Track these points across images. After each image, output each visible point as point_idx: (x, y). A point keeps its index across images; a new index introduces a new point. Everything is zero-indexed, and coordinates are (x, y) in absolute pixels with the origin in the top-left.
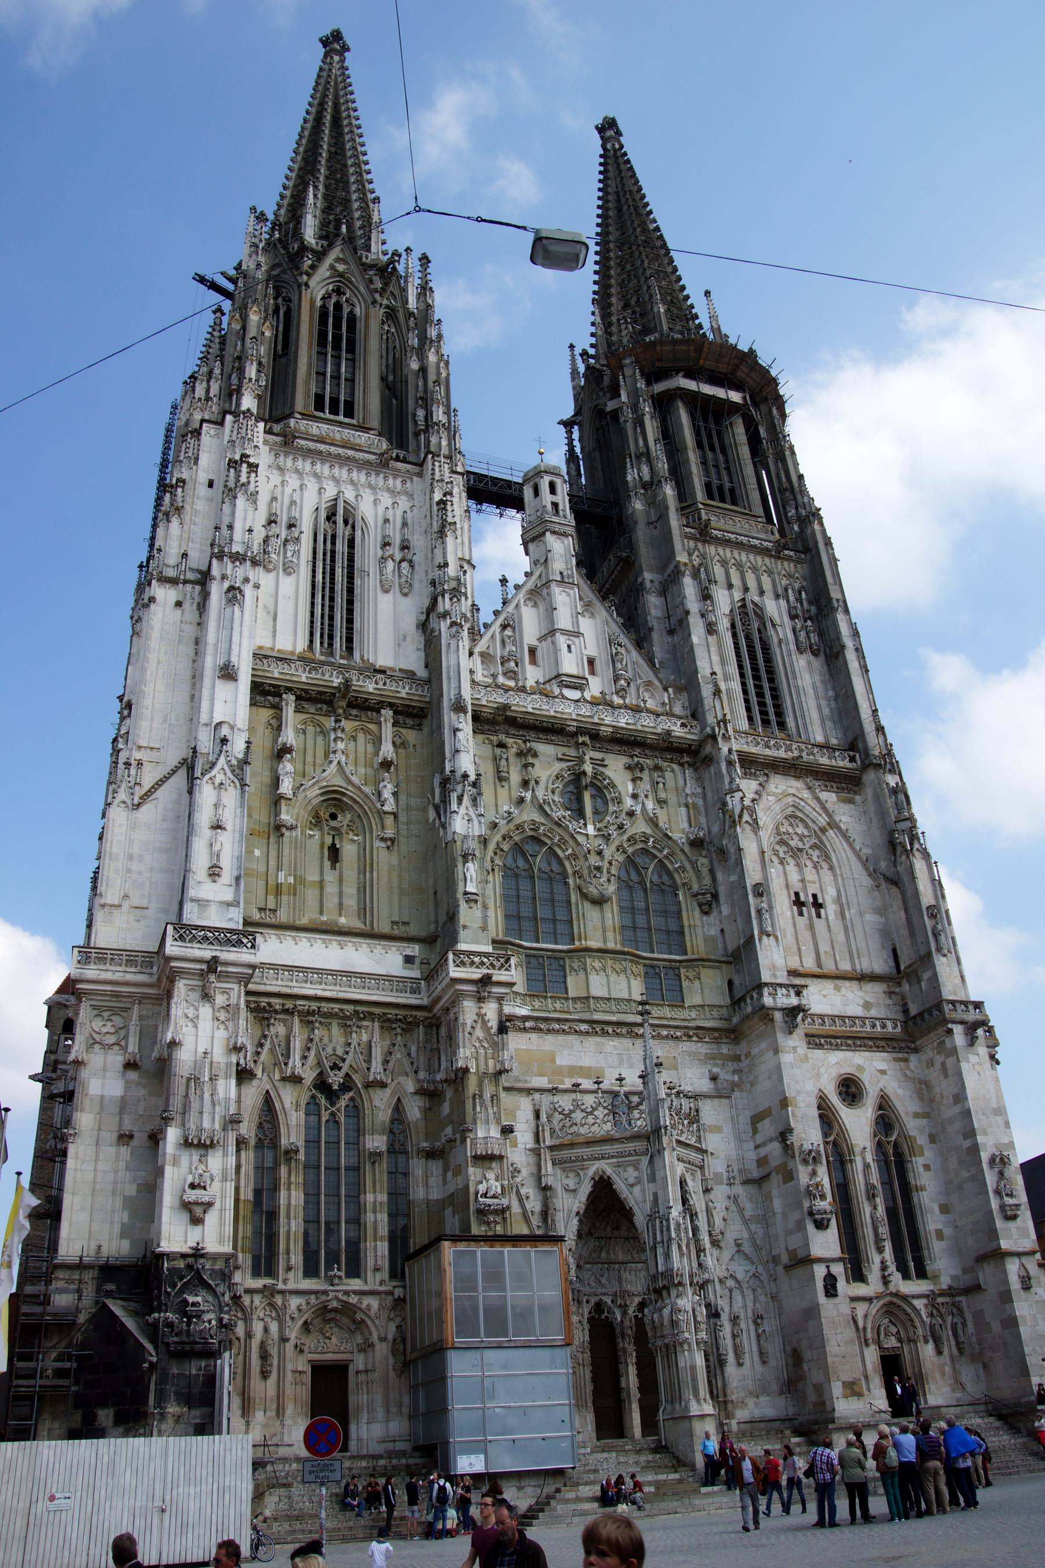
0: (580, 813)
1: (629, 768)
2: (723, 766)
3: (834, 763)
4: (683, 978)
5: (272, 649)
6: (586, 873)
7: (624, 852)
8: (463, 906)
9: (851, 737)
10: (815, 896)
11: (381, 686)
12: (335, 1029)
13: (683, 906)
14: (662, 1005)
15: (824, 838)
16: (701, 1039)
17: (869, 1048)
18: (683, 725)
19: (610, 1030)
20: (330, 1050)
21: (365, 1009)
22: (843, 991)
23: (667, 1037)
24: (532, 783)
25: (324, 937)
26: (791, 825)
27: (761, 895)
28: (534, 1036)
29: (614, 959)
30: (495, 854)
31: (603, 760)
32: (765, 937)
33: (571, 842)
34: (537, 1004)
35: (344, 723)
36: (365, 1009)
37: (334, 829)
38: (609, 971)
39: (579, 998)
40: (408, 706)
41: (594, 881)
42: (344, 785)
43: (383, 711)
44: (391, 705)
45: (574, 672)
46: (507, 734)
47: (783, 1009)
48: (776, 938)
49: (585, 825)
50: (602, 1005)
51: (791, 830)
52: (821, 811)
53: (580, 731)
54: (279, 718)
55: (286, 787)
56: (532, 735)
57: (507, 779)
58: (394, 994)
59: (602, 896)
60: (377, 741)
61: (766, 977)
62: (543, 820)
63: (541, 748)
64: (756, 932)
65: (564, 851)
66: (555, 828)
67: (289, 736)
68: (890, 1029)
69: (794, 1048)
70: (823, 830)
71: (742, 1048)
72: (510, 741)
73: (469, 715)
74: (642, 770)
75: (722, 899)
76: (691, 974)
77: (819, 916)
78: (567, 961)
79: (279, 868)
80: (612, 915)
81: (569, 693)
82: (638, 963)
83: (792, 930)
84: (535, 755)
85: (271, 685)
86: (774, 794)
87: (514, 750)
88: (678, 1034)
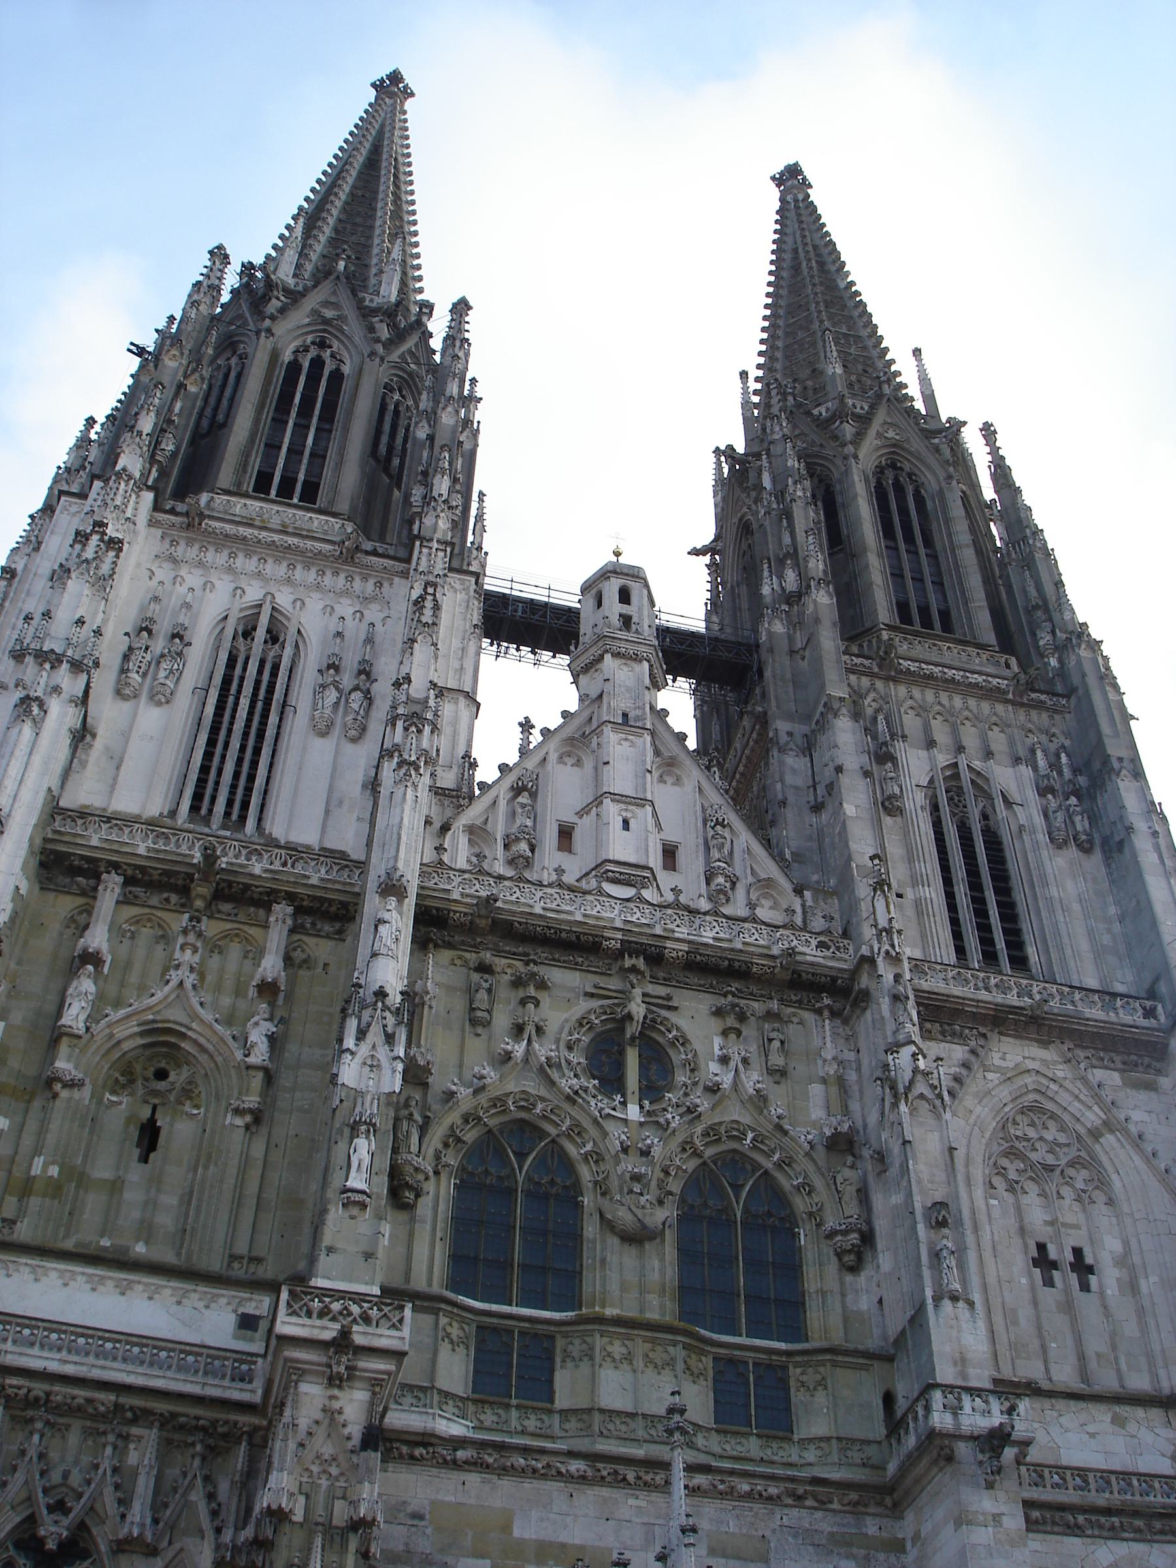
0: (613, 1083)
1: (718, 1013)
2: (885, 1004)
3: (1112, 1017)
4: (792, 1383)
5: (105, 810)
6: (614, 1183)
7: (696, 1154)
8: (336, 1214)
9: (1148, 978)
10: (1078, 1252)
11: (277, 866)
12: (74, 1438)
14: (743, 1435)
15: (1097, 1147)
16: (822, 1504)
18: (821, 945)
19: (631, 1476)
20: (56, 1477)
22: (1132, 1427)
23: (748, 1496)
24: (530, 1029)
25: (90, 1270)
26: (1032, 1124)
27: (942, 1224)
28: (474, 1479)
29: (653, 1341)
30: (446, 1145)
32: (947, 1304)
33: (593, 1132)
34: (489, 1418)
35: (205, 924)
37: (155, 1093)
38: (639, 1363)
39: (575, 1411)
40: (322, 900)
41: (628, 1199)
42: (184, 1019)
43: (276, 907)
44: (291, 897)
46: (498, 952)
47: (973, 1438)
48: (971, 1304)
49: (624, 1104)
50: (617, 1425)
51: (1031, 1133)
52: (1090, 1101)
53: (629, 948)
54: (88, 910)
55: (75, 1016)
56: (542, 953)
57: (487, 1024)
58: (200, 1378)
59: (644, 1227)
60: (256, 954)
61: (945, 1373)
62: (543, 1092)
63: (557, 976)
64: (929, 1293)
65: (580, 1146)
66: (566, 1106)
67: (98, 938)
70: (1095, 1134)
71: (905, 1528)
72: (500, 963)
73: (410, 902)
74: (742, 1017)
75: (881, 1243)
76: (810, 1377)
77: (1085, 1287)
78: (560, 1343)
79: (37, 1152)
82: (703, 1352)
85: (82, 857)
86: (998, 1070)
87: (507, 978)
88: (773, 1491)
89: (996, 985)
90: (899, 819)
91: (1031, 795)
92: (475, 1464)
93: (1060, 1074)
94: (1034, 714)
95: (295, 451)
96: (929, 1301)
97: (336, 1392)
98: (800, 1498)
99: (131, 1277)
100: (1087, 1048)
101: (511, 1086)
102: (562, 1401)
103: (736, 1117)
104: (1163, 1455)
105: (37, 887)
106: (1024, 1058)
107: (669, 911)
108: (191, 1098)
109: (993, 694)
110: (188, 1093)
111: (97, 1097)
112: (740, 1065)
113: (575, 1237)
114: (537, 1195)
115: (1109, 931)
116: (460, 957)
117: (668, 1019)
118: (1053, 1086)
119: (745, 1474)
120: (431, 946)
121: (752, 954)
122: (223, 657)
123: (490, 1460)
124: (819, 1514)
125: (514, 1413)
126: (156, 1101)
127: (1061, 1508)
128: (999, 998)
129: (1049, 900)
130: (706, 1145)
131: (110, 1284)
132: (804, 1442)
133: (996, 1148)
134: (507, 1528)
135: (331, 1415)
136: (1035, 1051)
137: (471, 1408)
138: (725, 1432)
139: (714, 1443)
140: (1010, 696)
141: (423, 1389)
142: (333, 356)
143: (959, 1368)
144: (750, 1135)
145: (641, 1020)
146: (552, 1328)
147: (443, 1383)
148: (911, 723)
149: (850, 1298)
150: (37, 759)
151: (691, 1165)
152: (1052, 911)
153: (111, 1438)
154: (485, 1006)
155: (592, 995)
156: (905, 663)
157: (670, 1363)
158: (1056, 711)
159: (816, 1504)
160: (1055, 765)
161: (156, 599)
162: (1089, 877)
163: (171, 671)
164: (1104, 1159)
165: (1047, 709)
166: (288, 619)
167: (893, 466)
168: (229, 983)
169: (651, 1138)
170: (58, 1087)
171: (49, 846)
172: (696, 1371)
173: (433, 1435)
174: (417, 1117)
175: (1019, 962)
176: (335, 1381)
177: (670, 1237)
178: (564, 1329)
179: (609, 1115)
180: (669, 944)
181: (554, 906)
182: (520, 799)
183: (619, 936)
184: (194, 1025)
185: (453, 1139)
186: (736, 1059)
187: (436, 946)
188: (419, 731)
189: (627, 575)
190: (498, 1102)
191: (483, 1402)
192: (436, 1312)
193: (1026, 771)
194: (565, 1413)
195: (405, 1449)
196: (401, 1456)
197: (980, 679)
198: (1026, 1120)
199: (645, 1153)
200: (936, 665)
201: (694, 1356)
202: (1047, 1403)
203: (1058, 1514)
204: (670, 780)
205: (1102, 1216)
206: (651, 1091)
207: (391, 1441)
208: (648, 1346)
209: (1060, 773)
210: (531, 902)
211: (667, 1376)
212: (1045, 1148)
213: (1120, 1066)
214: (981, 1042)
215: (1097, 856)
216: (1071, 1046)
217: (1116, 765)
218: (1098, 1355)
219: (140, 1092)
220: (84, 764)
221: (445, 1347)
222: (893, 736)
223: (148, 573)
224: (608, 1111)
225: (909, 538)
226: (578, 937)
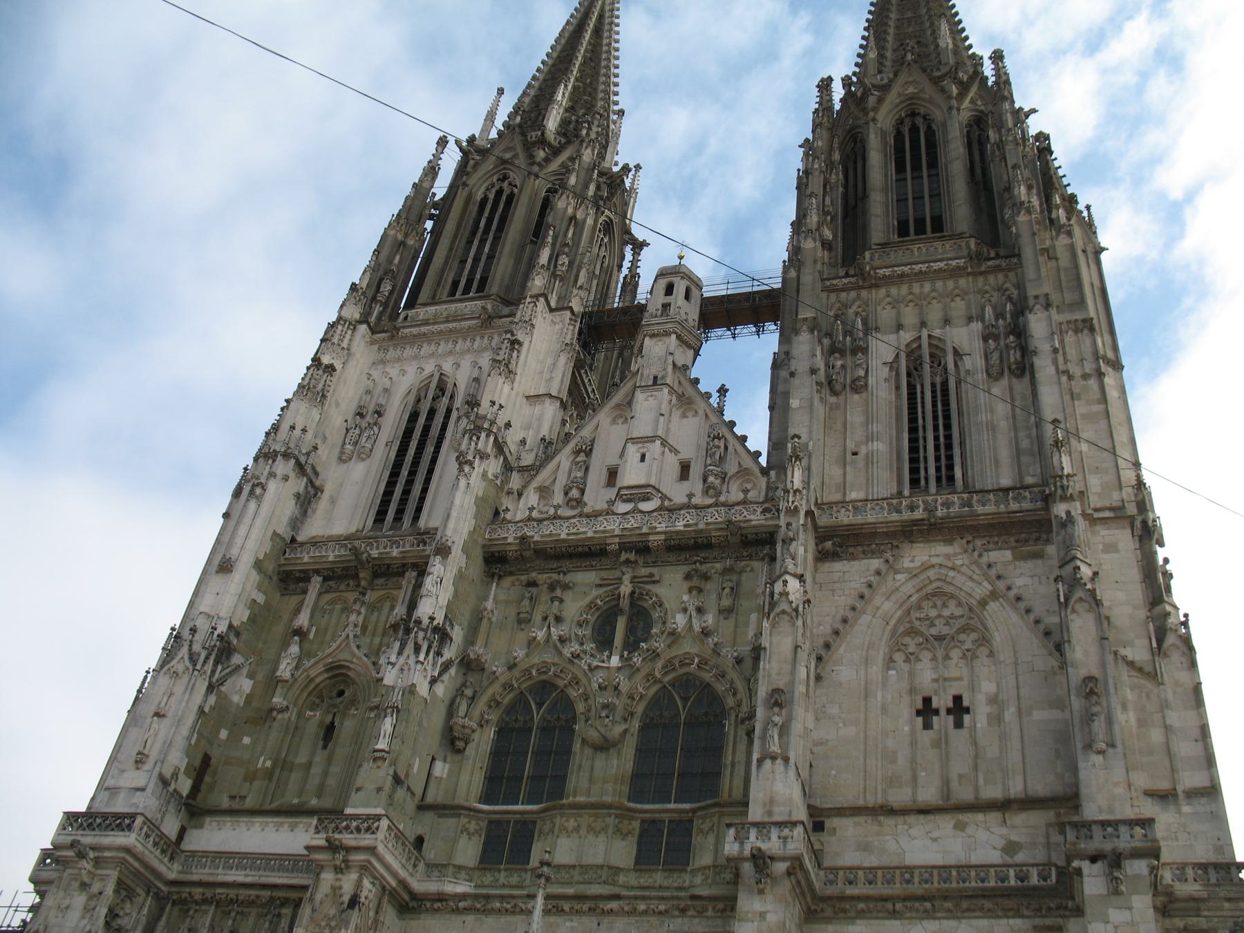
7: (656, 681)
10: (958, 699)
11: (408, 548)
16: (701, 913)
17: (989, 914)
18: (764, 511)
19: (566, 908)
21: (282, 894)
22: (970, 830)
23: (645, 912)
25: (275, 820)
26: (935, 606)
27: (777, 704)
29: (597, 816)
31: (652, 575)
34: (488, 879)
36: (282, 894)
38: (583, 831)
45: (642, 481)
46: (542, 571)
49: (609, 657)
50: (564, 875)
51: (933, 613)
53: (624, 547)
54: (302, 603)
55: (285, 669)
62: (556, 660)
64: (755, 756)
66: (569, 666)
67: (303, 620)
68: (1034, 880)
69: (762, 915)
70: (983, 603)
74: (706, 577)
77: (959, 724)
78: (538, 826)
80: (622, 762)
81: (623, 507)
82: (632, 818)
84: (566, 587)
85: (300, 571)
86: (908, 570)
88: (662, 908)
90: (864, 395)
91: (978, 345)
92: (471, 909)
93: (958, 562)
94: (991, 278)
95: (476, 260)
96: (755, 762)
97: (340, 876)
98: (683, 911)
99: (297, 820)
100: (985, 536)
101: (536, 660)
103: (687, 650)
104: (995, 848)
105: (278, 595)
106: (930, 556)
107: (655, 514)
108: (353, 705)
109: (954, 273)
110: (353, 702)
111: (300, 715)
112: (694, 614)
113: (568, 752)
114: (546, 729)
115: (1029, 436)
116: (518, 580)
117: (649, 590)
118: (951, 574)
119: (643, 898)
120: (496, 577)
121: (711, 530)
122: (406, 417)
123: (478, 906)
124: (697, 920)
125: (503, 873)
126: (335, 710)
127: (884, 899)
128: (906, 515)
131: (271, 825)
132: (694, 872)
133: (901, 629)
135: (336, 890)
136: (942, 549)
137: (477, 874)
138: (641, 871)
139: (633, 879)
140: (969, 270)
141: (444, 866)
142: (510, 184)
143: (767, 808)
144: (696, 660)
145: (627, 594)
146: (535, 816)
147: (459, 860)
148: (885, 315)
150: (259, 522)
151: (653, 691)
153: (269, 917)
154: (528, 609)
155: (601, 586)
156: (881, 272)
157: (604, 829)
158: (1009, 270)
159: (695, 913)
160: (999, 315)
161: (368, 392)
163: (369, 437)
164: (989, 623)
165: (1002, 270)
166: (448, 377)
167: (913, 114)
168: (380, 630)
170: (275, 713)
171: (281, 569)
172: (625, 831)
173: (444, 894)
175: (946, 479)
176: (338, 870)
178: (542, 815)
179: (597, 667)
180: (651, 538)
181: (575, 531)
183: (617, 540)
184: (354, 660)
185: (494, 703)
186: (692, 609)
187: (500, 577)
188: (478, 438)
189: (671, 274)
190: (527, 671)
191: (485, 869)
192: (459, 816)
193: (977, 326)
195: (428, 905)
196: (427, 910)
197: (942, 265)
198: (931, 604)
199: (616, 688)
200: (906, 265)
201: (626, 822)
202: (900, 819)
203: (880, 904)
204: (690, 414)
206: (631, 645)
207: (422, 900)
208: (592, 819)
209: (1004, 319)
210: (559, 532)
211: (602, 838)
212: (943, 621)
213: (1014, 544)
216: (970, 538)
217: (1031, 302)
218: (960, 776)
219: (325, 705)
220: (314, 511)
222: (867, 330)
223: (366, 376)
224: (595, 663)
225: (916, 167)
226: (590, 548)
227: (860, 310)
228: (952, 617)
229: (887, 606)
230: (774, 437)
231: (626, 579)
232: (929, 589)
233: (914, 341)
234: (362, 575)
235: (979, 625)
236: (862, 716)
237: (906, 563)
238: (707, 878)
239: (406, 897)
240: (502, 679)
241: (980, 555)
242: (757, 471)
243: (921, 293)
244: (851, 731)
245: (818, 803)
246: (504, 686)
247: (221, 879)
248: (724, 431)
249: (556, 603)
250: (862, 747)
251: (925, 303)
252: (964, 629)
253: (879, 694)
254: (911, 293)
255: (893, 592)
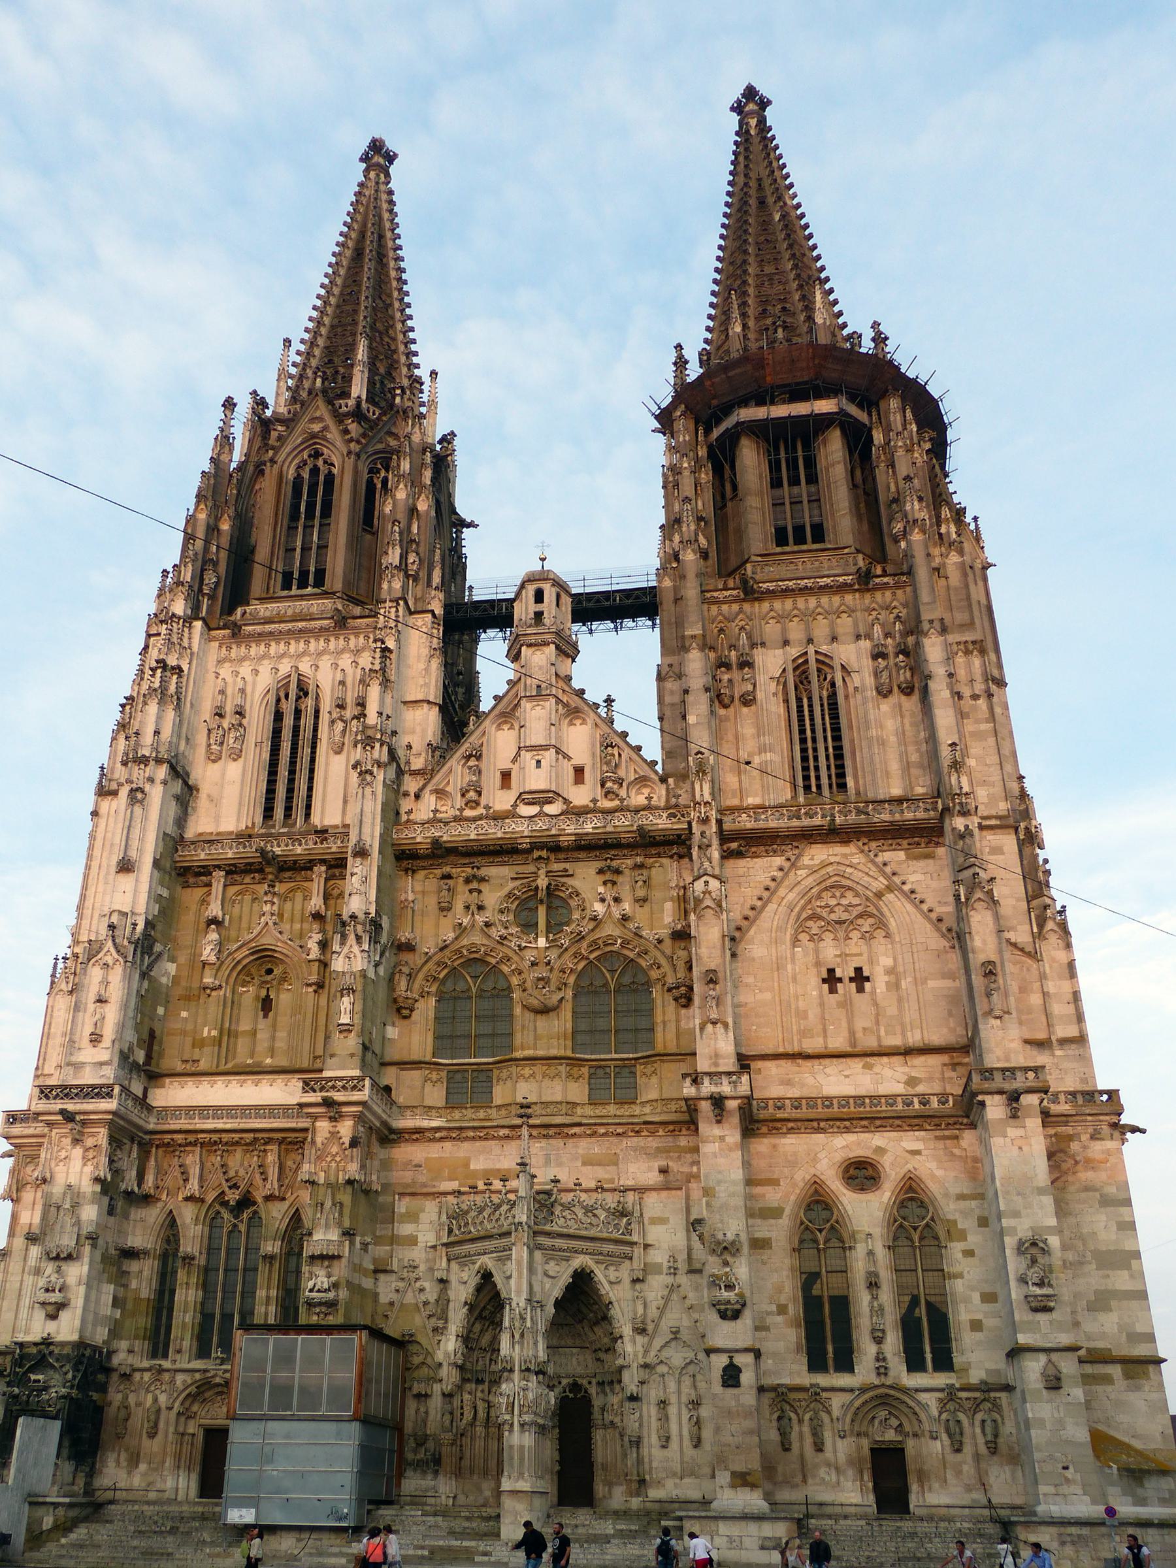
13: (659, 1002)
26: (834, 896)
46: (455, 866)
62: (485, 942)
66: (499, 947)
70: (879, 895)
77: (861, 990)
78: (496, 1072)
80: (563, 1021)
83: (818, 1010)
89: (806, 814)
91: (867, 663)
93: (855, 861)
101: (465, 942)
102: (498, 1100)
118: (849, 870)
120: (410, 873)
123: (454, 1135)
129: (870, 739)
130: (591, 952)
132: (643, 1103)
134: (467, 1165)
139: (588, 1110)
149: (683, 1024)
152: (870, 747)
162: (907, 714)
164: (885, 910)
169: (553, 955)
174: (406, 970)
177: (568, 1007)
182: (470, 763)
187: (414, 871)
192: (421, 1069)
193: (866, 645)
194: (499, 1107)
205: (880, 944)
214: (796, 852)
215: (916, 697)
221: (428, 1085)
227: (743, 623)
228: (850, 905)
229: (791, 896)
230: (666, 746)
231: (542, 872)
232: (828, 883)
233: (800, 656)
234: (268, 870)
235: (875, 912)
236: (776, 984)
237: (806, 860)
238: (655, 1109)
239: (386, 1132)
240: (436, 958)
241: (876, 855)
242: (656, 778)
243: (807, 609)
244: (767, 996)
245: (743, 1051)
246: (438, 964)
247: (199, 1127)
248: (617, 740)
249: (475, 894)
250: (778, 1008)
251: (811, 619)
252: (860, 916)
253: (789, 967)
254: (796, 608)
255: (796, 885)
